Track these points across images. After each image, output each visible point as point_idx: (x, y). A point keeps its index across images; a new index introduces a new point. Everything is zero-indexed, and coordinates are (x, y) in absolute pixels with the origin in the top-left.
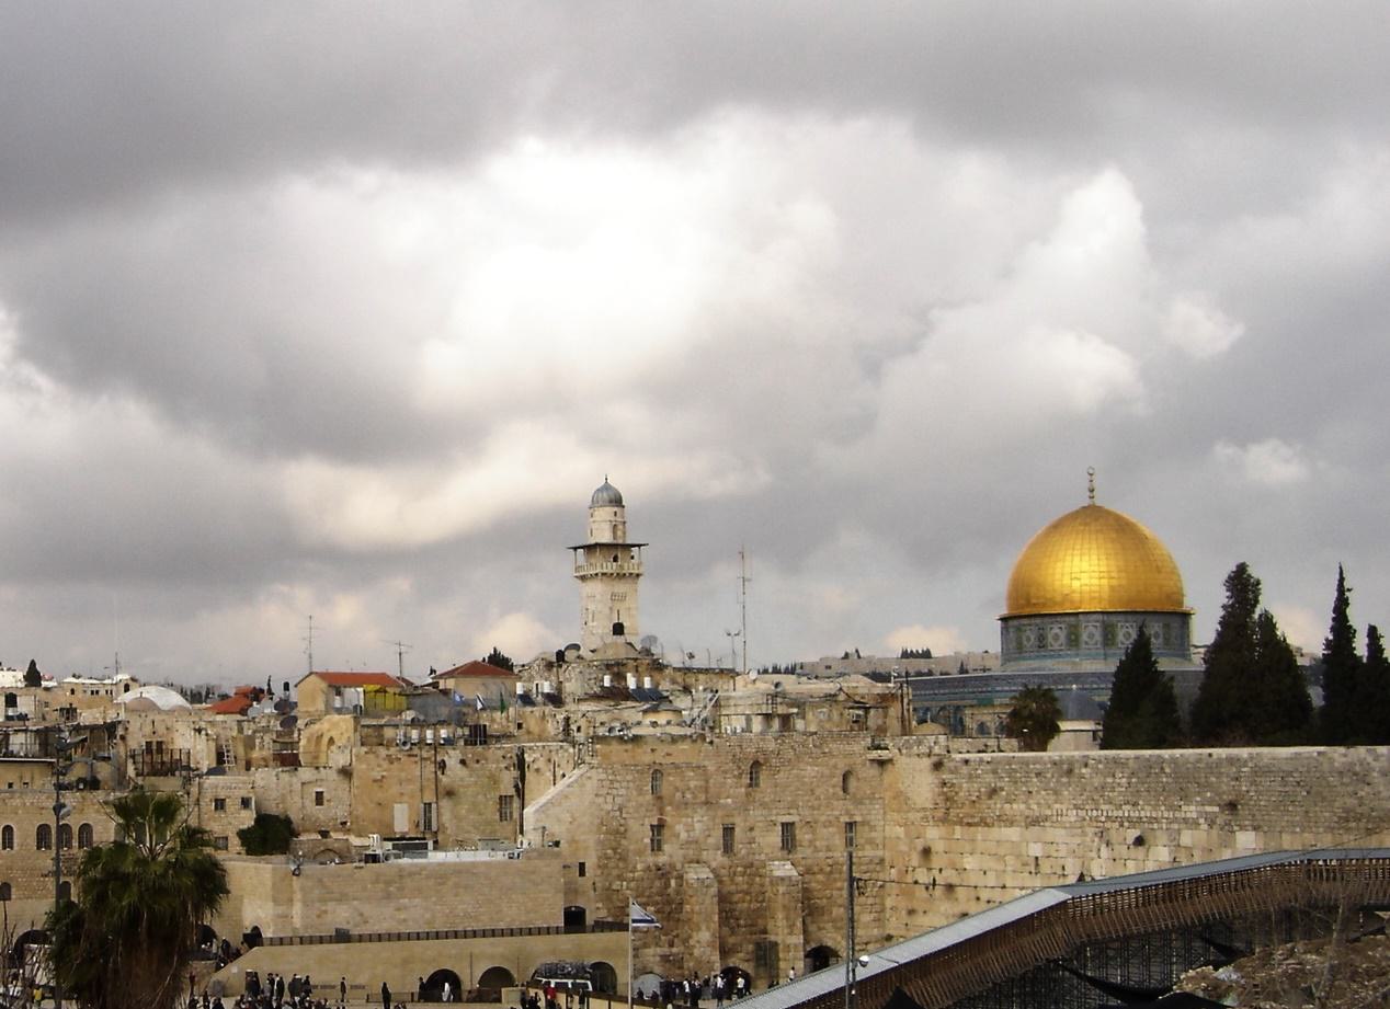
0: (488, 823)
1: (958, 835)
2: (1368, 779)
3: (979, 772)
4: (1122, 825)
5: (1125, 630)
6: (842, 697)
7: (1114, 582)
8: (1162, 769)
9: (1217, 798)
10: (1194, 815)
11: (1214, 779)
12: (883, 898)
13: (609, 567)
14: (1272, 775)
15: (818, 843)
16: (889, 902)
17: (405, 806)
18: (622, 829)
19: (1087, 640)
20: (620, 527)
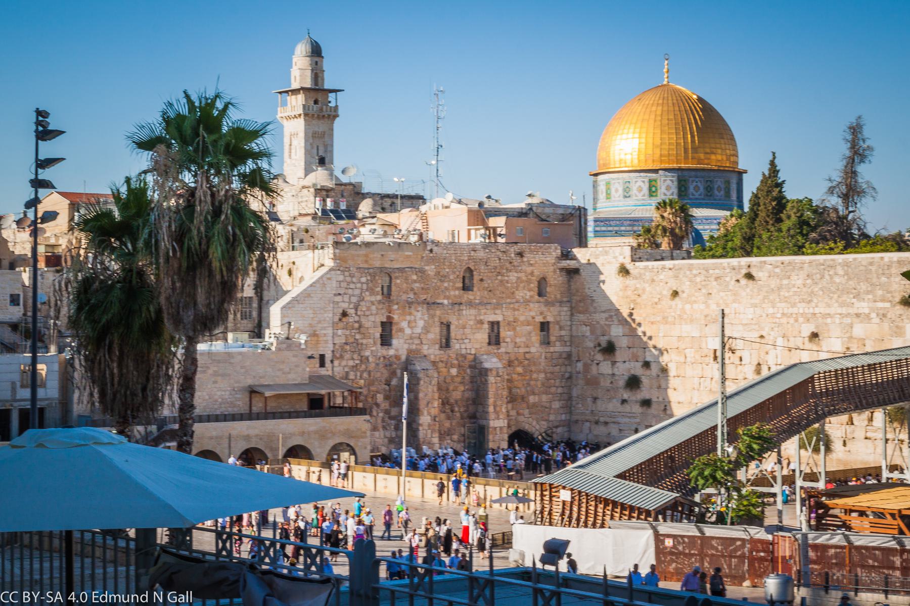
3: (662, 277)
4: (796, 321)
5: (695, 184)
6: (531, 215)
8: (836, 274)
9: (889, 295)
10: (867, 311)
11: (884, 279)
12: (570, 388)
15: (518, 340)
16: (575, 393)
18: (356, 325)
20: (320, 75)
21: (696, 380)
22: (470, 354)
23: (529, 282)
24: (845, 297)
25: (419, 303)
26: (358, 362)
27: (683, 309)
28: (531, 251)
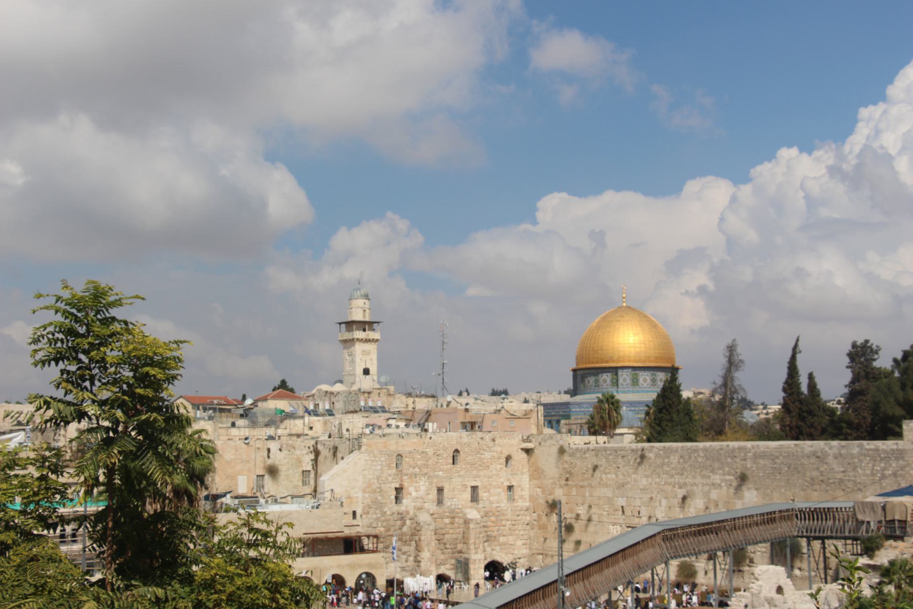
0: (295, 487)
1: (574, 493)
2: (826, 461)
5: (643, 377)
6: (503, 412)
7: (638, 350)
8: (699, 456)
9: (733, 471)
10: (718, 481)
11: (729, 460)
13: (361, 335)
14: (766, 457)
17: (245, 477)
18: (378, 490)
19: (623, 383)
20: (368, 311)
21: (611, 527)
22: (458, 508)
23: (499, 458)
24: (704, 472)
25: (422, 475)
26: (379, 515)
27: (601, 479)
28: (501, 437)
